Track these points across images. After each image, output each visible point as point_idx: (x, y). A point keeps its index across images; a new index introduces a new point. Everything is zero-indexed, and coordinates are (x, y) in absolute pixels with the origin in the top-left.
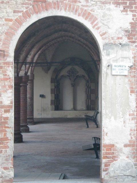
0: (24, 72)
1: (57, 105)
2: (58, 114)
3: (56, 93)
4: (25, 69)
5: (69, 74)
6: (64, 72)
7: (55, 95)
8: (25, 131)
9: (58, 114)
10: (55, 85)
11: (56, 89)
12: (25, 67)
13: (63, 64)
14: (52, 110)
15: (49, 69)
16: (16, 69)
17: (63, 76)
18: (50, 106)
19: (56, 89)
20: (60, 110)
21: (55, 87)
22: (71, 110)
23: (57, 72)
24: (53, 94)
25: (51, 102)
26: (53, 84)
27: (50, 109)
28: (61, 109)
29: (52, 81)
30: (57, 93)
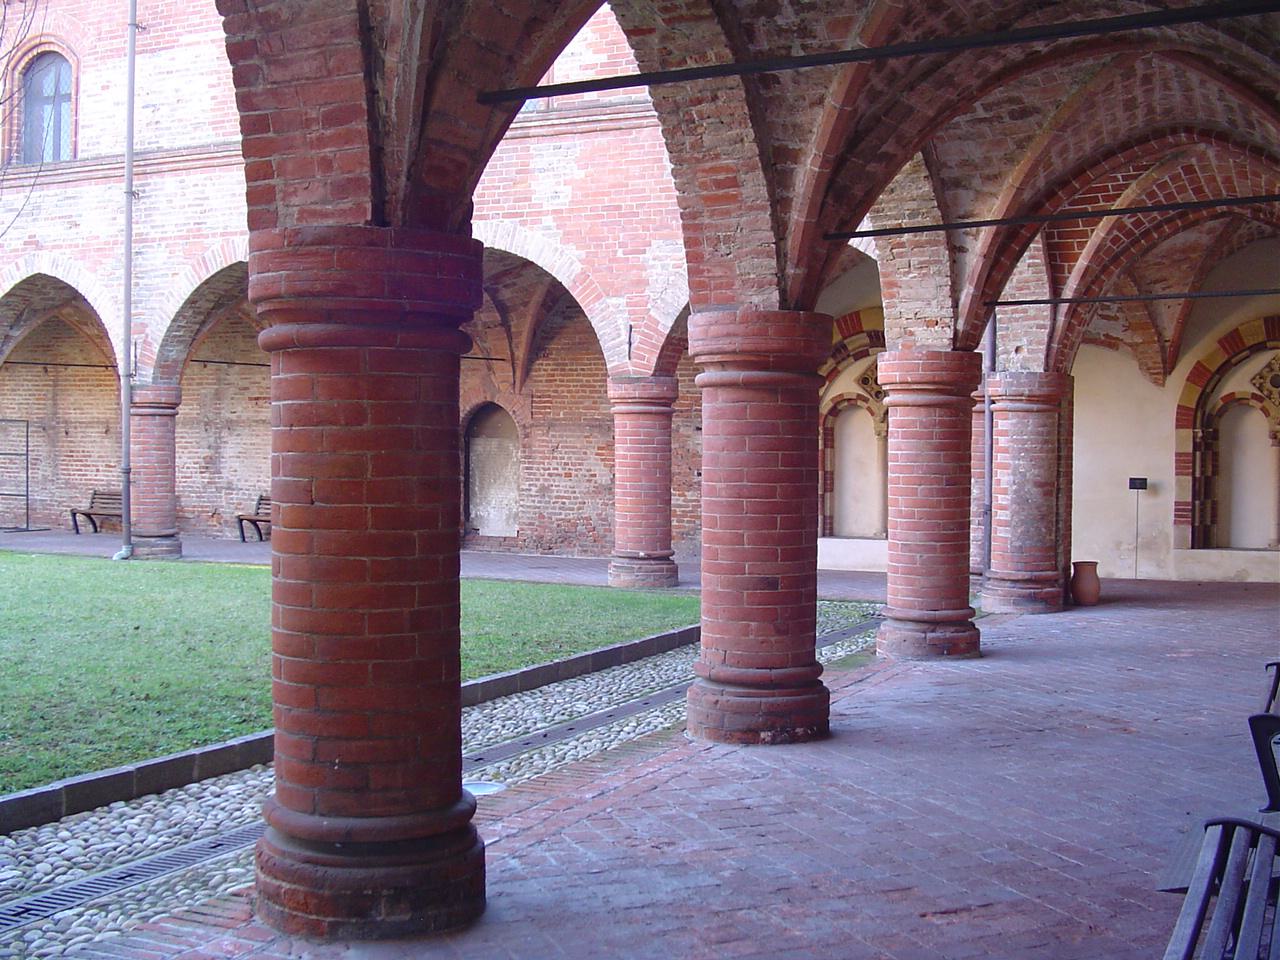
0: (950, 333)
1: (1206, 523)
2: (1211, 565)
3: (1198, 475)
4: (956, 317)
5: (1260, 389)
6: (1239, 383)
7: (1194, 480)
8: (948, 654)
9: (1211, 565)
10: (1194, 438)
11: (1198, 453)
12: (955, 305)
13: (1236, 349)
14: (1178, 546)
15: (1168, 367)
16: (774, 263)
17: (1231, 399)
18: (1170, 528)
19: (1198, 453)
20: (1218, 547)
21: (1196, 446)
22: (1265, 550)
23: (1206, 379)
24: (1187, 474)
25: (1176, 510)
26: (1188, 433)
27: (1172, 541)
28: (1225, 545)
29: (1185, 417)
30: (1202, 473)
